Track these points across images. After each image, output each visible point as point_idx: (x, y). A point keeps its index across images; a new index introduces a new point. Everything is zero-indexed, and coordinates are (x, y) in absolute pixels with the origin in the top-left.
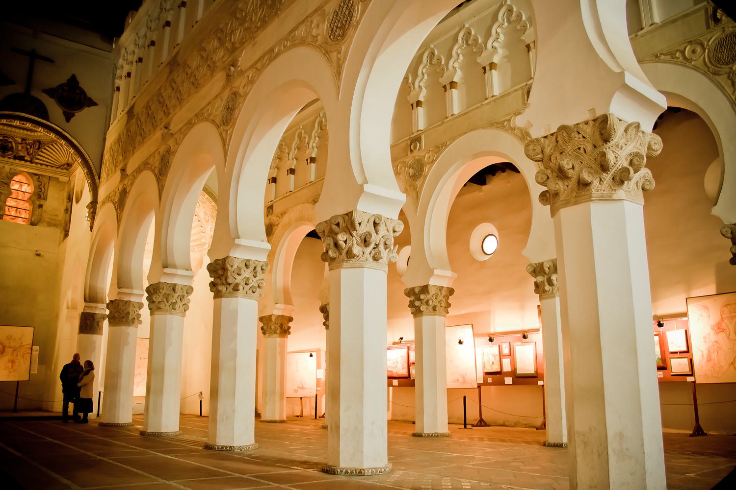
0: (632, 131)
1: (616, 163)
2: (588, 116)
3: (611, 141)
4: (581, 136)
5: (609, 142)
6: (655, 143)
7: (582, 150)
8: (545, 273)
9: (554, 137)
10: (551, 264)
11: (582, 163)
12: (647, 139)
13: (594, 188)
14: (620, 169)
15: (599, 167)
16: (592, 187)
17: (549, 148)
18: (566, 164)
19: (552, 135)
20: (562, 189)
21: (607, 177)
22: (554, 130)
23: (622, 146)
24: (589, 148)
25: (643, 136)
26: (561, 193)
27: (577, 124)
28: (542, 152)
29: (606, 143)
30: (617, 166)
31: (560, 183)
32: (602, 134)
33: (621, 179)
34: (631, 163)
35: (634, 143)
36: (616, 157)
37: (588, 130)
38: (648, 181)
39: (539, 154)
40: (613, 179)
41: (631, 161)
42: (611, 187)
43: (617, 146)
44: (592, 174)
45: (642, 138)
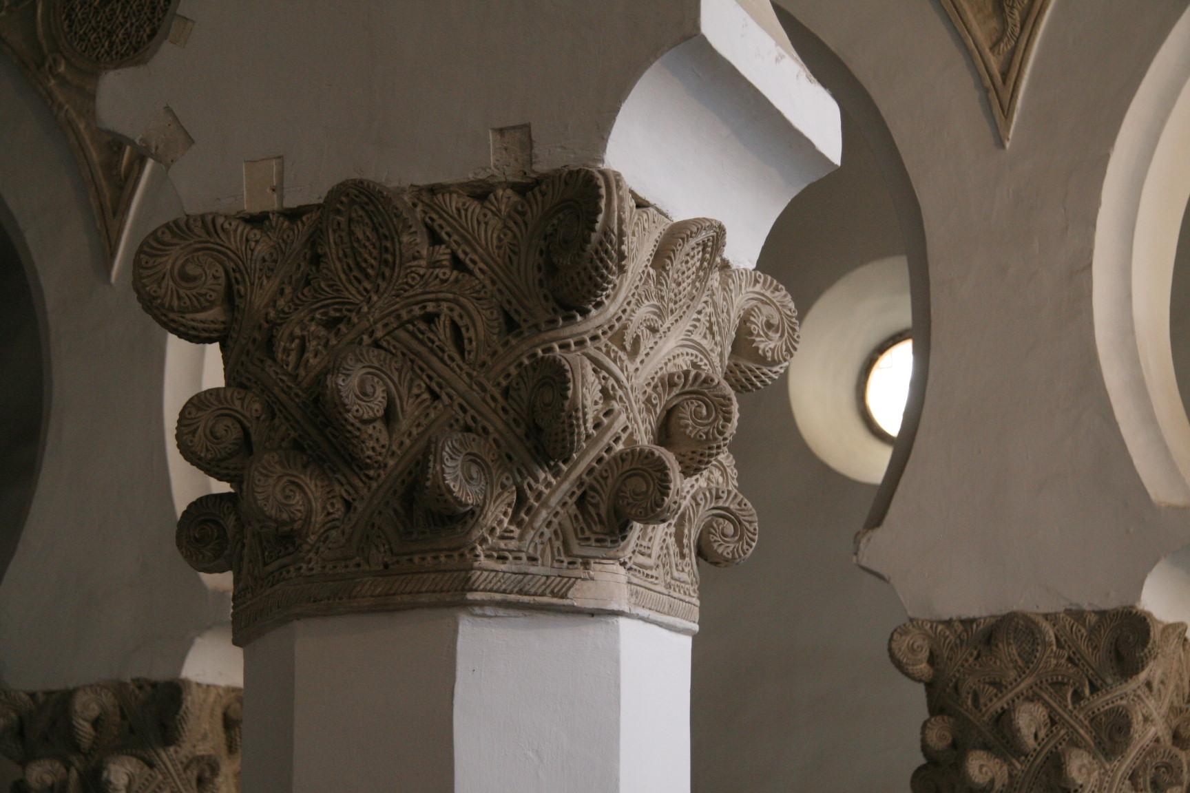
0: (686, 261)
1: (606, 421)
2: (493, 161)
3: (594, 312)
4: (443, 253)
5: (585, 313)
6: (769, 325)
7: (443, 333)
8: (77, 749)
9: (303, 228)
10: (108, 699)
11: (435, 397)
12: (741, 299)
13: (483, 540)
14: (622, 457)
15: (520, 431)
16: (477, 534)
17: (270, 286)
18: (360, 389)
19: (293, 215)
20: (318, 518)
21: (555, 490)
22: (307, 191)
23: (636, 341)
24: (482, 326)
25: (725, 286)
26: (312, 539)
27: (433, 190)
28: (230, 297)
29: (570, 319)
30: (607, 439)
31: (313, 487)
32: (552, 269)
33: (618, 503)
34: (665, 432)
35: (686, 324)
36: (604, 391)
37: (487, 230)
38: (727, 514)
39: (212, 304)
40: (581, 502)
41: (670, 414)
42: (565, 543)
43: (618, 338)
44: (484, 467)
45: (719, 297)
